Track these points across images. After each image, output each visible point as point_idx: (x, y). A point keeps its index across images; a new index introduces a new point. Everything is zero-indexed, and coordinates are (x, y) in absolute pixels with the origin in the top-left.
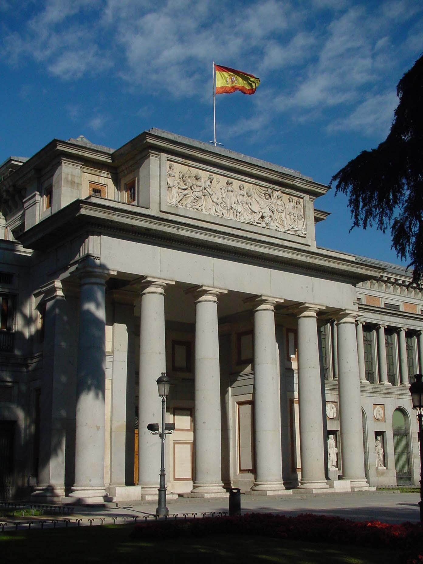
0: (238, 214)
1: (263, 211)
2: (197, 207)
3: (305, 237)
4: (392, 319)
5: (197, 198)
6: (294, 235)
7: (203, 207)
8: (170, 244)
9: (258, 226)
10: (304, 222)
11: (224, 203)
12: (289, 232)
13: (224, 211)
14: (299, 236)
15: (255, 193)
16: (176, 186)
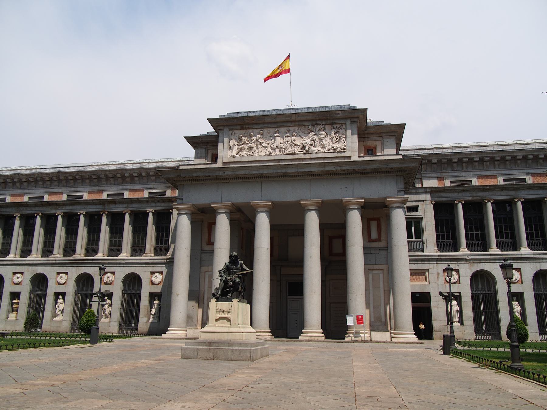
0: (283, 150)
1: (303, 142)
2: (250, 154)
3: (344, 152)
4: (531, 192)
5: (251, 148)
6: (333, 152)
7: (256, 152)
8: (228, 181)
9: (300, 154)
10: (345, 141)
11: (272, 145)
12: (329, 151)
13: (272, 151)
14: (338, 152)
15: (300, 132)
16: (236, 144)
